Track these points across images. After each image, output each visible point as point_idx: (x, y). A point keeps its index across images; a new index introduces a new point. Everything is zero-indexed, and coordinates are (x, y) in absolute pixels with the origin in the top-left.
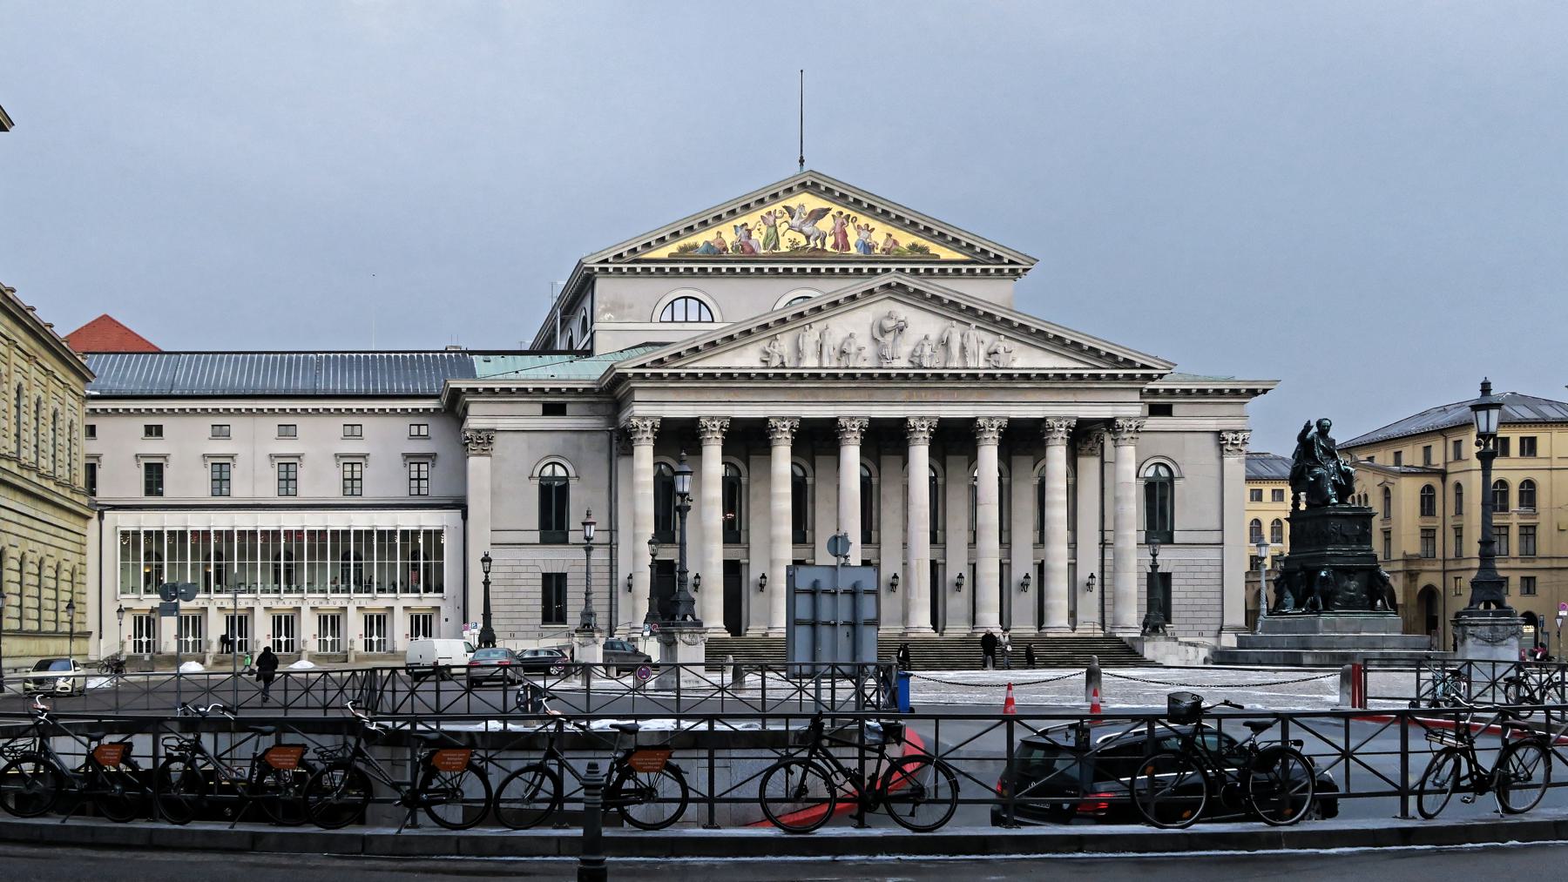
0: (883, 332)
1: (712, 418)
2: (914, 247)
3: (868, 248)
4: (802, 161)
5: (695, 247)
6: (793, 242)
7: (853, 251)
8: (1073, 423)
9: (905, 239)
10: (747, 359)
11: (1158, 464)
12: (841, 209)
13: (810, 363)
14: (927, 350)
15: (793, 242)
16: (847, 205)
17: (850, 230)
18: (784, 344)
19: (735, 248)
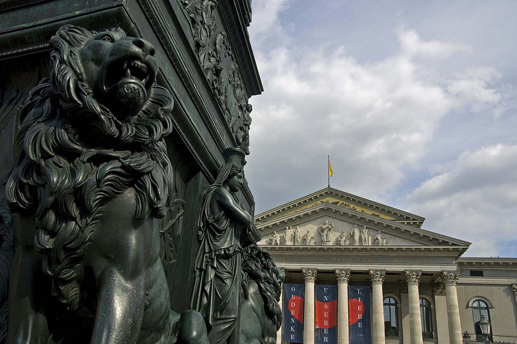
0: (323, 230)
9: (369, 212)
12: (343, 202)
13: (289, 243)
14: (344, 239)
16: (345, 200)
18: (277, 237)
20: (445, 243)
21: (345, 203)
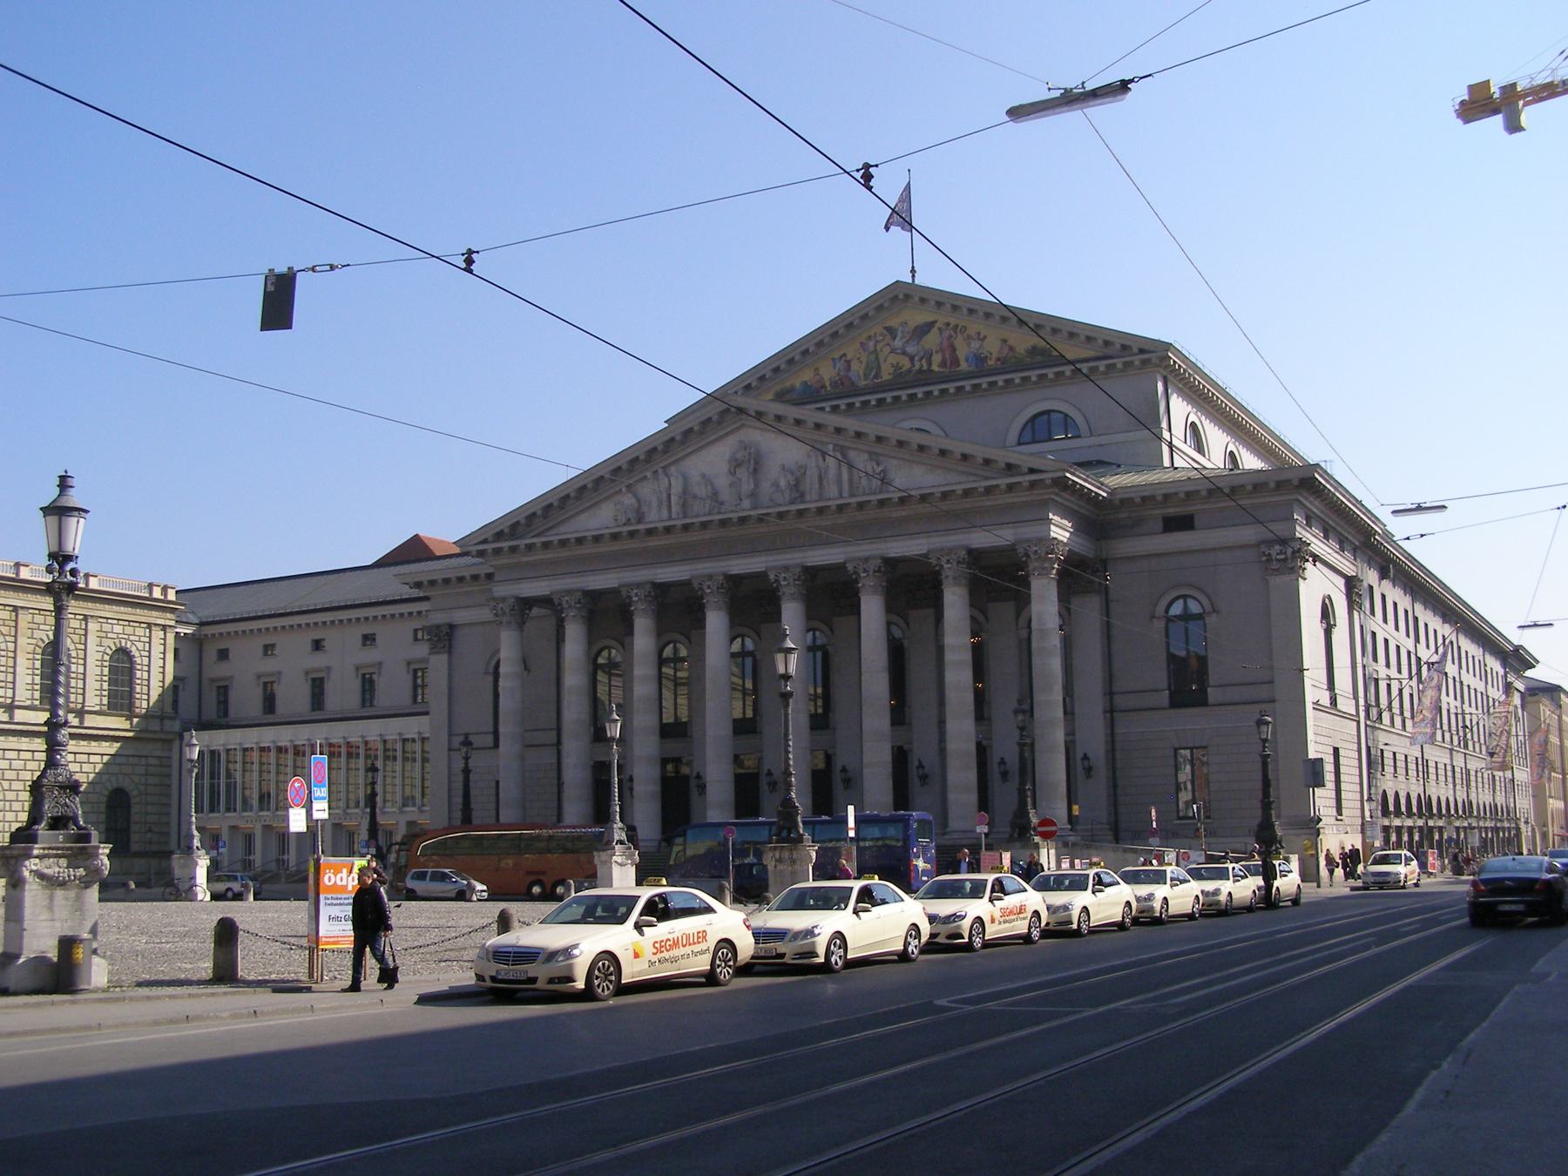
1: (569, 592)
2: (1034, 351)
3: (980, 360)
4: (913, 271)
5: (792, 389)
6: (897, 367)
7: (964, 366)
8: (963, 553)
10: (602, 518)
11: (1185, 597)
13: (655, 517)
15: (897, 367)
17: (959, 342)
19: (834, 384)
20: (1010, 468)
21: (953, 321)
